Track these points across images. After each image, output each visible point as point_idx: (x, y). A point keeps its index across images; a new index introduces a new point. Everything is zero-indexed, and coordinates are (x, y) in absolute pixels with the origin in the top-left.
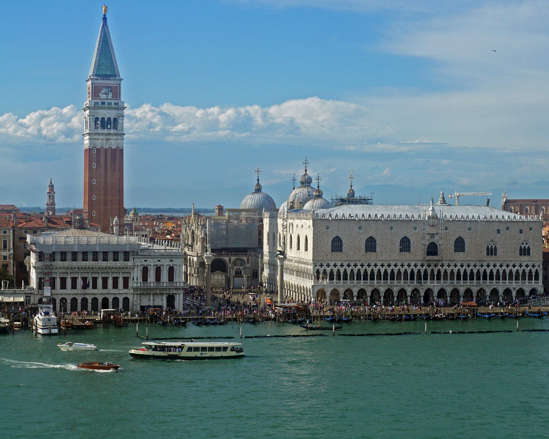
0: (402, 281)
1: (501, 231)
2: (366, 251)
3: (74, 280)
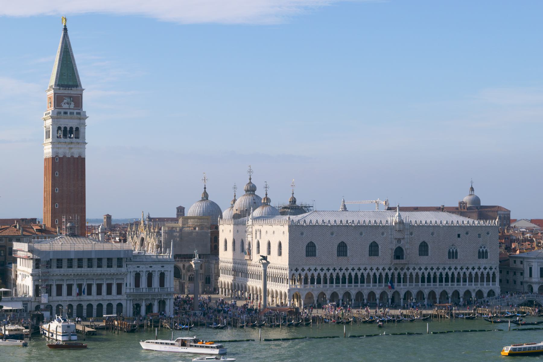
0: (371, 284)
1: (461, 236)
3: (70, 287)
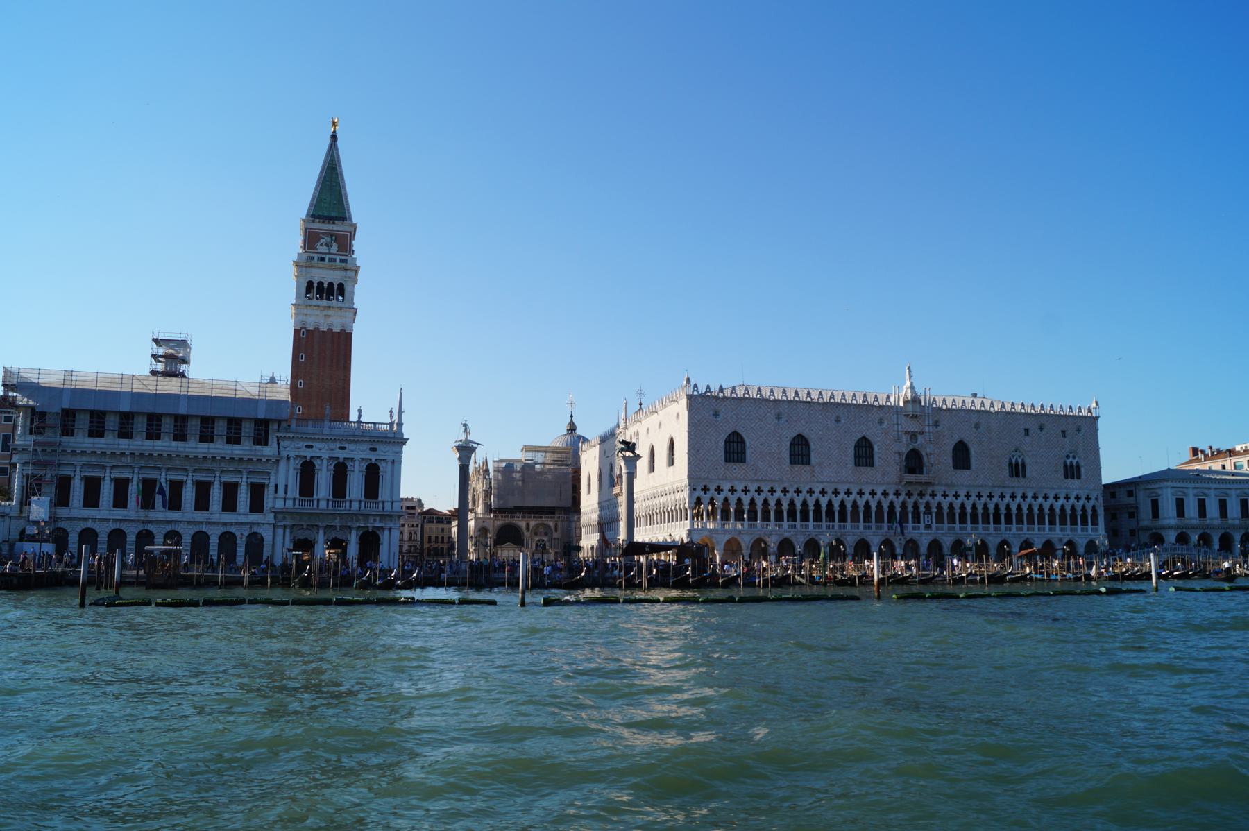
0: (861, 524)
3: (121, 487)
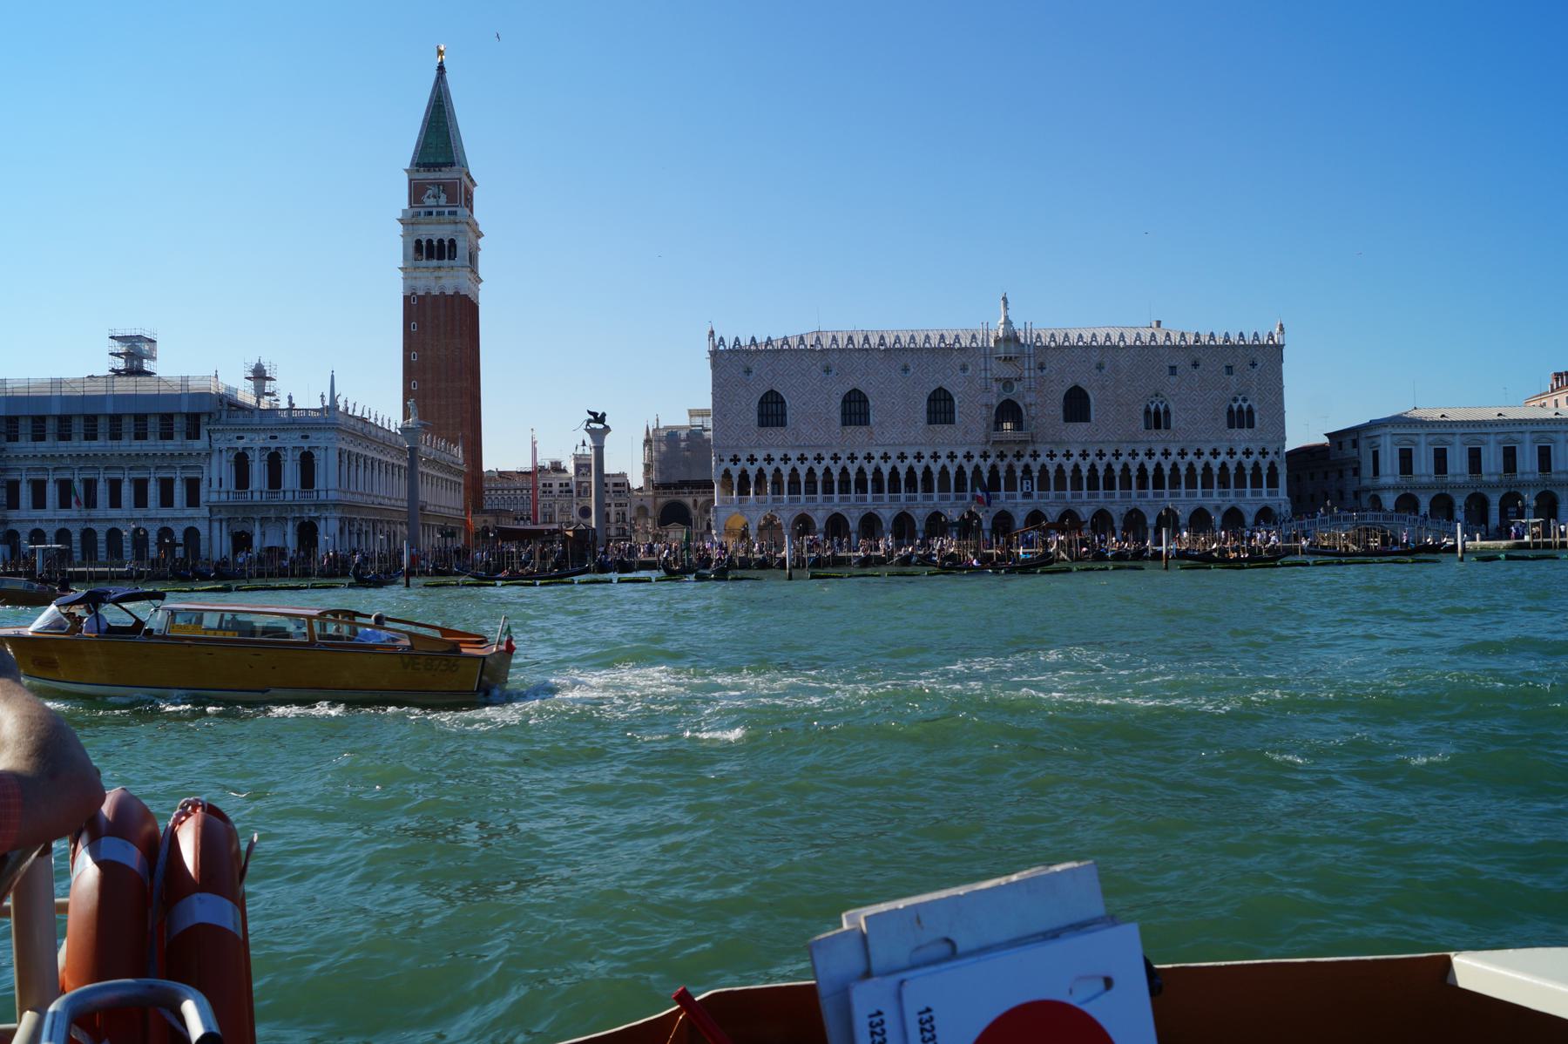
0: (936, 494)
2: (844, 424)
